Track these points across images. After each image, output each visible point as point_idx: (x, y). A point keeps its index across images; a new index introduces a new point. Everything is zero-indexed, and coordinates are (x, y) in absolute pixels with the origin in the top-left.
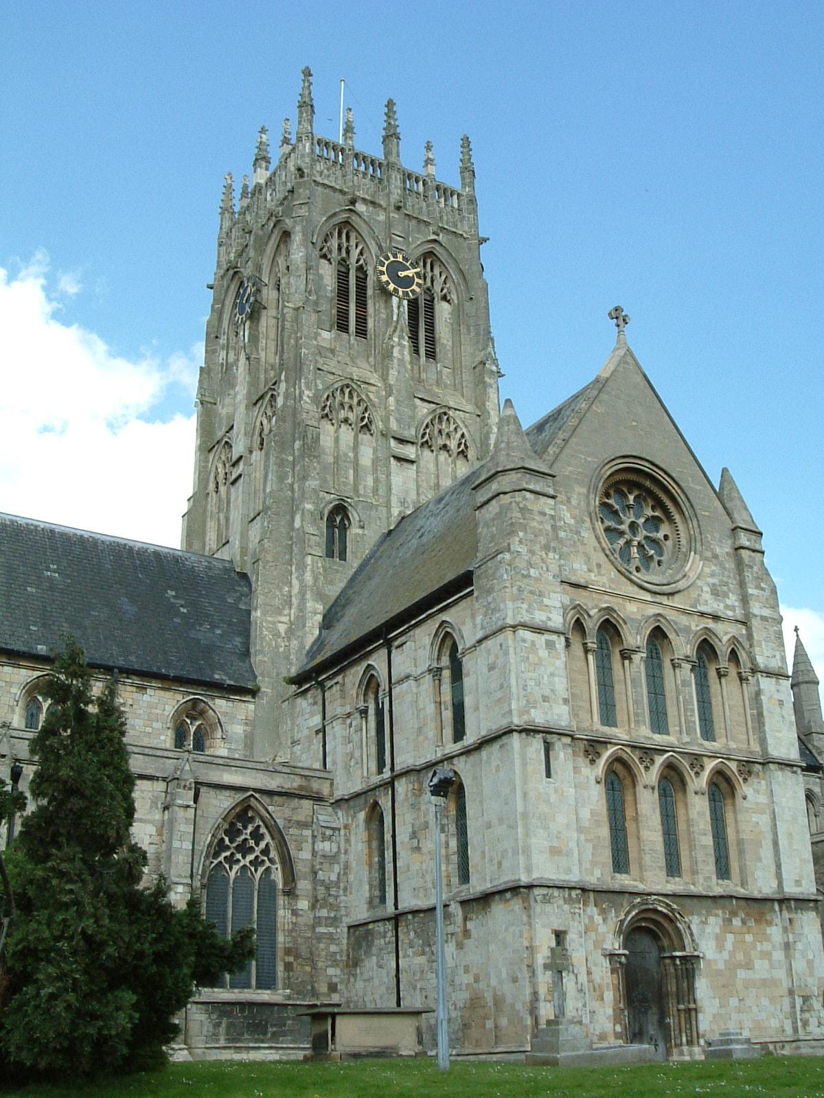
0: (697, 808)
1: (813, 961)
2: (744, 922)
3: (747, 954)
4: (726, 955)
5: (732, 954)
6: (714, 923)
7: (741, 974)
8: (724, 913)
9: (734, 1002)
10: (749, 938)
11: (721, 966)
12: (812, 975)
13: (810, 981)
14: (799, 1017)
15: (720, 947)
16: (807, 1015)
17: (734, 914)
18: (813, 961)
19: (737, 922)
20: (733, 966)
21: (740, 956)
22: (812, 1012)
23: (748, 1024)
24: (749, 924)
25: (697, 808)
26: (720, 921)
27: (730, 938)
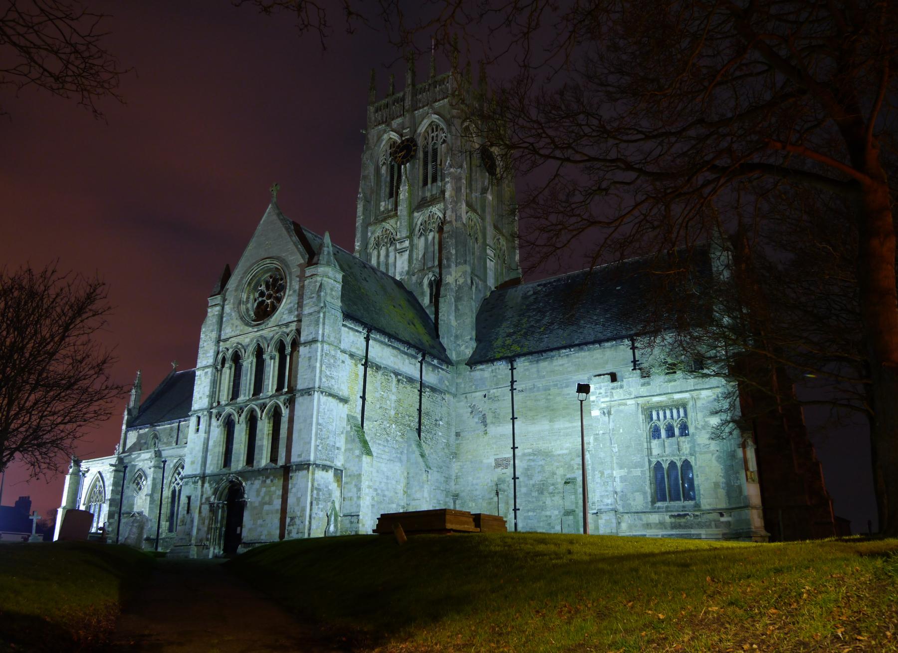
0: (264, 427)
1: (300, 498)
2: (272, 481)
3: (271, 497)
4: (260, 499)
5: (263, 498)
6: (257, 483)
7: (266, 507)
8: (263, 478)
9: (260, 522)
10: (273, 489)
11: (257, 504)
12: (298, 505)
13: (296, 509)
14: (287, 528)
15: (258, 492)
16: (291, 528)
17: (267, 477)
18: (300, 498)
19: (268, 481)
20: (263, 504)
21: (267, 499)
22: (295, 526)
23: (265, 532)
24: (274, 481)
25: (264, 427)
26: (260, 482)
27: (264, 490)
